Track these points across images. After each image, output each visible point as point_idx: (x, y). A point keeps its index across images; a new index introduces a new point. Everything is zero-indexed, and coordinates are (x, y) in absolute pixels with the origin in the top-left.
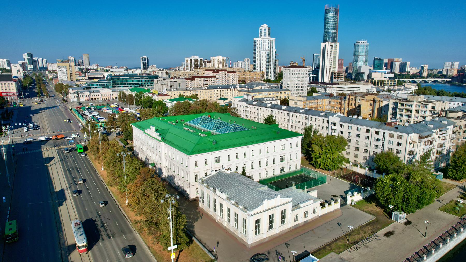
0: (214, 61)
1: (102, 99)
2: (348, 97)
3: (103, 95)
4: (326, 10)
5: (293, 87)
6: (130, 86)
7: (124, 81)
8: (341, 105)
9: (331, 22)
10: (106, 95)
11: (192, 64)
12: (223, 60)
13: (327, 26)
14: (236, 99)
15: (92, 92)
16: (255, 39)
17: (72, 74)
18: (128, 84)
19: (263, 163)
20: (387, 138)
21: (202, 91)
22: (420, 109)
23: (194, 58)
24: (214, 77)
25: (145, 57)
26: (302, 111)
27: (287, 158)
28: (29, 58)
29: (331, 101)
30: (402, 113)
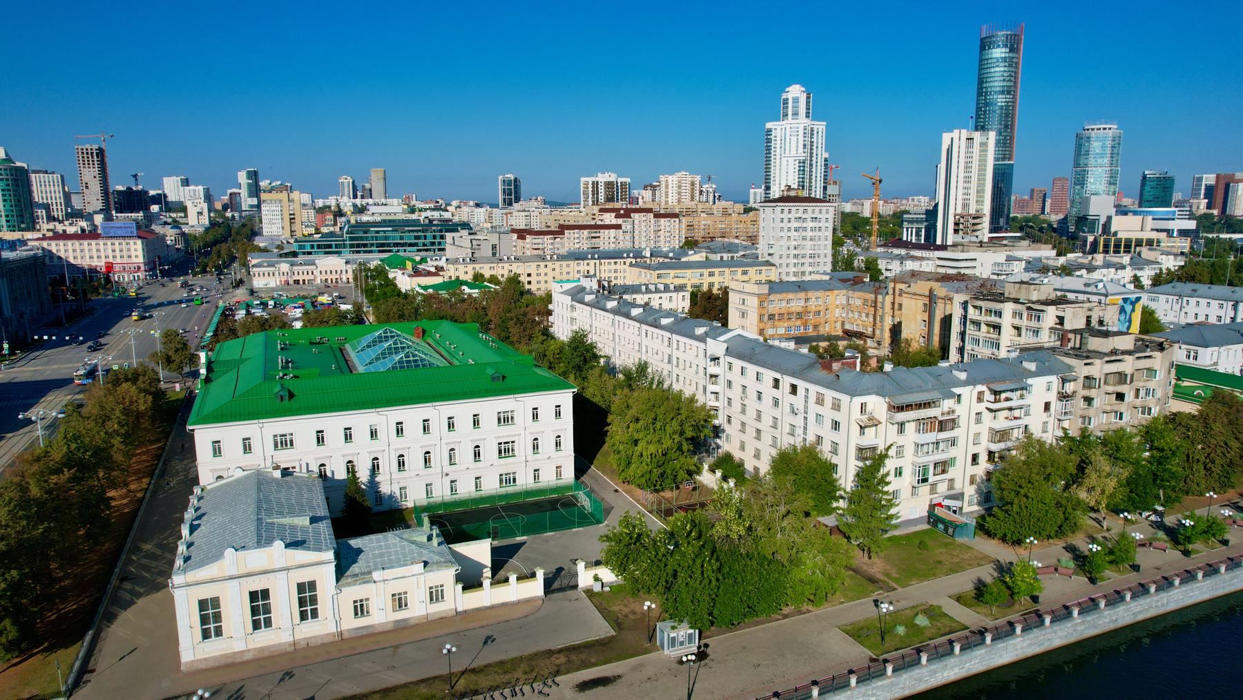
0: (667, 187)
1: (321, 282)
2: (891, 285)
3: (324, 273)
4: (982, 40)
5: (785, 256)
6: (395, 249)
7: (381, 238)
8: (875, 307)
9: (998, 74)
10: (326, 272)
11: (598, 194)
12: (693, 184)
13: (984, 85)
15: (298, 265)
16: (769, 125)
17: (294, 219)
18: (389, 245)
19: (439, 458)
20: (814, 408)
21: (542, 264)
22: (1024, 322)
23: (603, 178)
24: (618, 227)
25: (509, 176)
26: (664, 321)
27: (523, 447)
28: (251, 181)
29: (853, 296)
30: (978, 333)
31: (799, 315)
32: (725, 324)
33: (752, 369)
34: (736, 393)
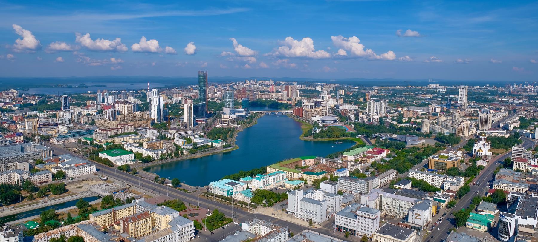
12: (131, 106)
27: (131, 157)
32: (143, 147)
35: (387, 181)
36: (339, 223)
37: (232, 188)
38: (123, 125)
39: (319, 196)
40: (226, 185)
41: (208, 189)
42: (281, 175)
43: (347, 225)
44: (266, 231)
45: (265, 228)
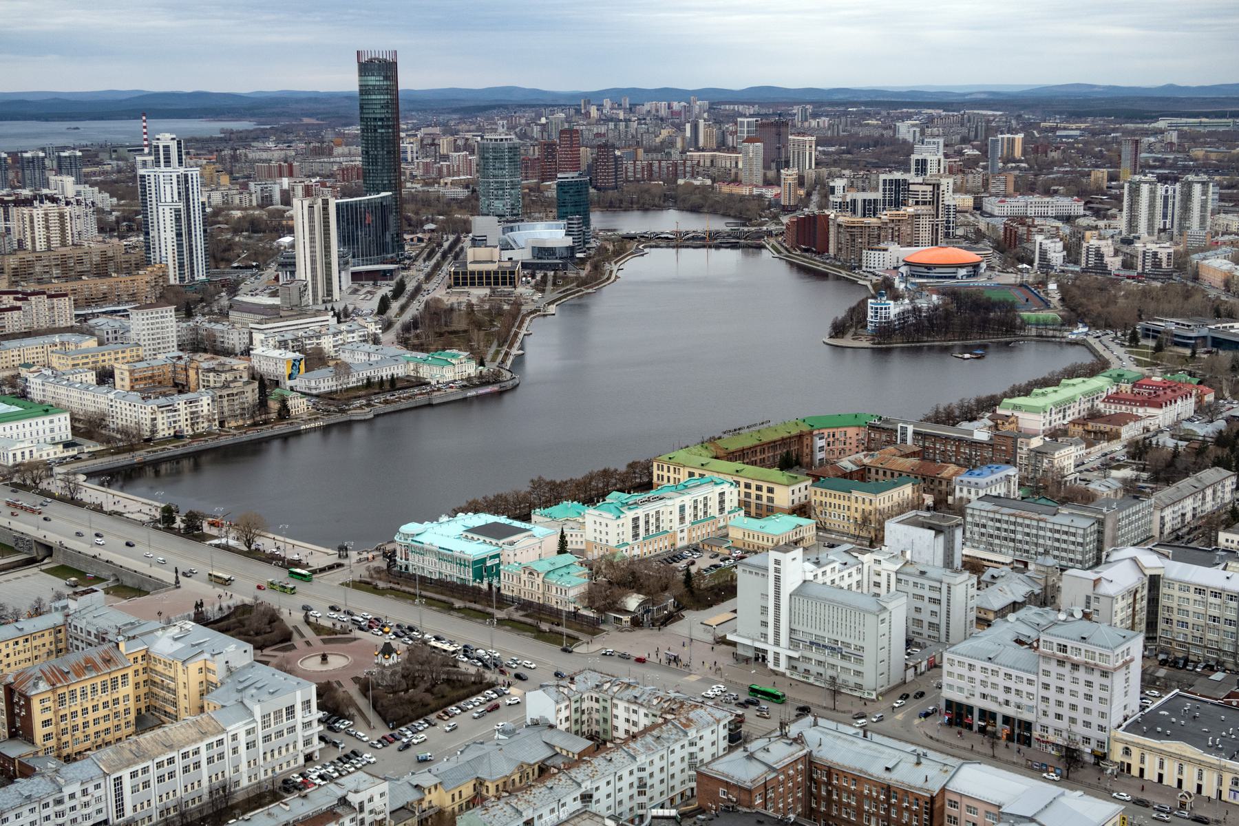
14: (31, 375)
19: (34, 433)
24: (19, 308)
27: (56, 430)
31: (150, 378)
33: (123, 402)
34: (118, 410)
35: (1189, 517)
36: (961, 689)
37: (491, 550)
38: (25, 296)
39: (877, 579)
40: (470, 535)
41: (390, 556)
42: (718, 489)
43: (995, 699)
44: (635, 724)
45: (627, 709)
